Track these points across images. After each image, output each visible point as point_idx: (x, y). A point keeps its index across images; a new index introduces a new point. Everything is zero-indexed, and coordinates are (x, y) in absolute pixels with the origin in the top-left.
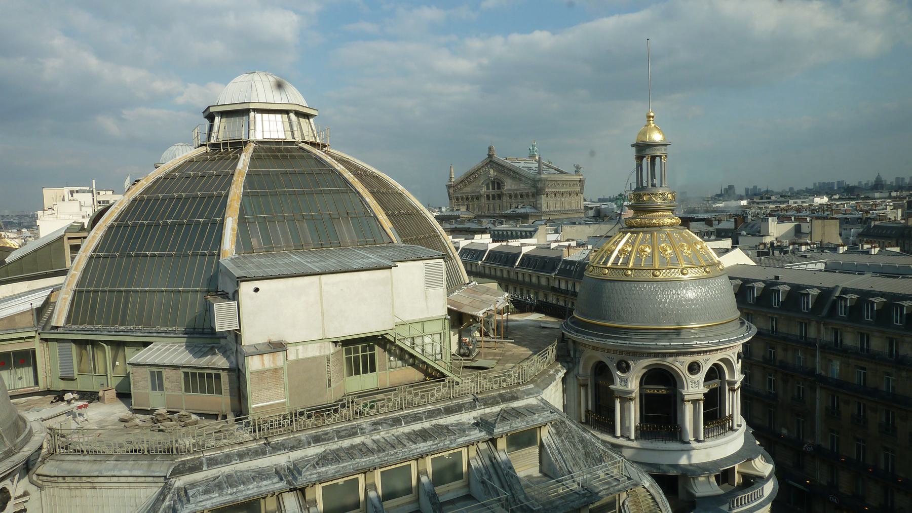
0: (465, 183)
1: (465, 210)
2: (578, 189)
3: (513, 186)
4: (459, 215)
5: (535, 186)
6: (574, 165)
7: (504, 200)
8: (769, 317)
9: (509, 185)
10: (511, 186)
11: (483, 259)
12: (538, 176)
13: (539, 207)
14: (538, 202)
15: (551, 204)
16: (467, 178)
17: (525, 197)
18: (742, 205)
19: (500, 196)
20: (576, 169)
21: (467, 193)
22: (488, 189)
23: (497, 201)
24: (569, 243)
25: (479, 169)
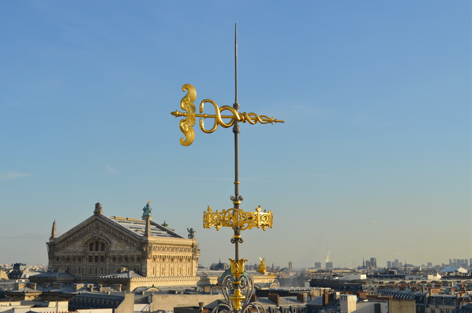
0: (67, 242)
1: (64, 272)
2: (190, 254)
4: (56, 277)
5: (140, 249)
6: (188, 229)
7: (107, 263)
10: (116, 248)
12: (145, 239)
14: (143, 267)
15: (158, 269)
16: (70, 236)
17: (130, 260)
18: (362, 278)
19: (103, 259)
20: (189, 234)
21: (68, 252)
22: (91, 250)
25: (84, 227)
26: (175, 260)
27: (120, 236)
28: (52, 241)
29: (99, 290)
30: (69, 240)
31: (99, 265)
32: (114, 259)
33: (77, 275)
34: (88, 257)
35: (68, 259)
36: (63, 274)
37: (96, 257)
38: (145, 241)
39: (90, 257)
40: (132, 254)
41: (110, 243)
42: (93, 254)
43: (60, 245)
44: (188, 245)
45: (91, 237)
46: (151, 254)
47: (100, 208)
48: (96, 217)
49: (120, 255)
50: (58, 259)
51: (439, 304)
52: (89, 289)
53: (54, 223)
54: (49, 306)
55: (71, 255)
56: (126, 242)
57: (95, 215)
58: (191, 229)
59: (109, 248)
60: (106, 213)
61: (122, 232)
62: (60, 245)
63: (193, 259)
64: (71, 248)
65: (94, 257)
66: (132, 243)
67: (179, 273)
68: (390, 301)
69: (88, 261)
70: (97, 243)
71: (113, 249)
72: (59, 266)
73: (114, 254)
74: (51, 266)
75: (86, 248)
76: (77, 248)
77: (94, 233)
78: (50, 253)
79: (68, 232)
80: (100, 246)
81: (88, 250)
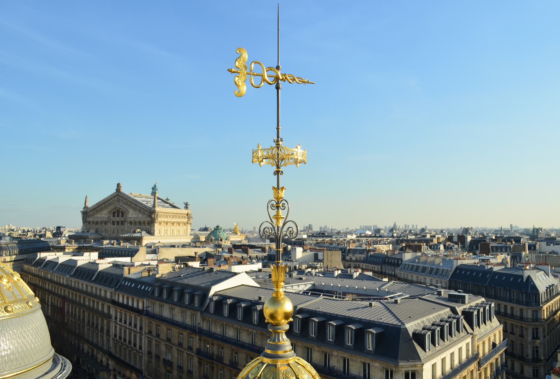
0: (96, 210)
1: (94, 232)
2: (186, 220)
3: (134, 215)
4: (88, 236)
7: (126, 226)
8: (250, 332)
9: (132, 215)
10: (132, 215)
11: (72, 274)
12: (153, 209)
13: (152, 233)
14: (152, 229)
15: (163, 230)
16: (98, 207)
18: (304, 237)
19: (122, 223)
20: (185, 206)
21: (97, 218)
22: (114, 216)
23: (121, 227)
24: (149, 262)
25: (109, 200)
26: (175, 224)
27: (135, 207)
28: (85, 210)
29: (120, 245)
30: (97, 210)
31: (119, 227)
32: (131, 223)
33: (104, 234)
34: (111, 221)
35: (97, 223)
36: (94, 233)
37: (118, 222)
38: (153, 210)
39: (113, 222)
40: (144, 220)
41: (128, 211)
42: (116, 219)
43: (91, 213)
44: (184, 214)
45: (114, 207)
46: (158, 220)
47: (120, 187)
48: (117, 193)
49: (135, 220)
50: (89, 223)
51: (355, 253)
52: (113, 244)
53: (86, 197)
54: (84, 255)
55: (99, 220)
56: (140, 211)
57: (116, 192)
58: (187, 203)
59: (127, 215)
60: (125, 190)
61: (137, 204)
62: (91, 213)
63: (187, 223)
64: (99, 215)
65: (116, 222)
66: (144, 212)
67: (178, 233)
68: (324, 251)
69: (111, 224)
70: (118, 212)
71: (130, 216)
72: (91, 228)
73: (131, 220)
74: (84, 228)
75: (110, 215)
76: (104, 215)
77: (116, 205)
78: (83, 219)
79: (97, 204)
80: (120, 214)
81: (112, 217)
